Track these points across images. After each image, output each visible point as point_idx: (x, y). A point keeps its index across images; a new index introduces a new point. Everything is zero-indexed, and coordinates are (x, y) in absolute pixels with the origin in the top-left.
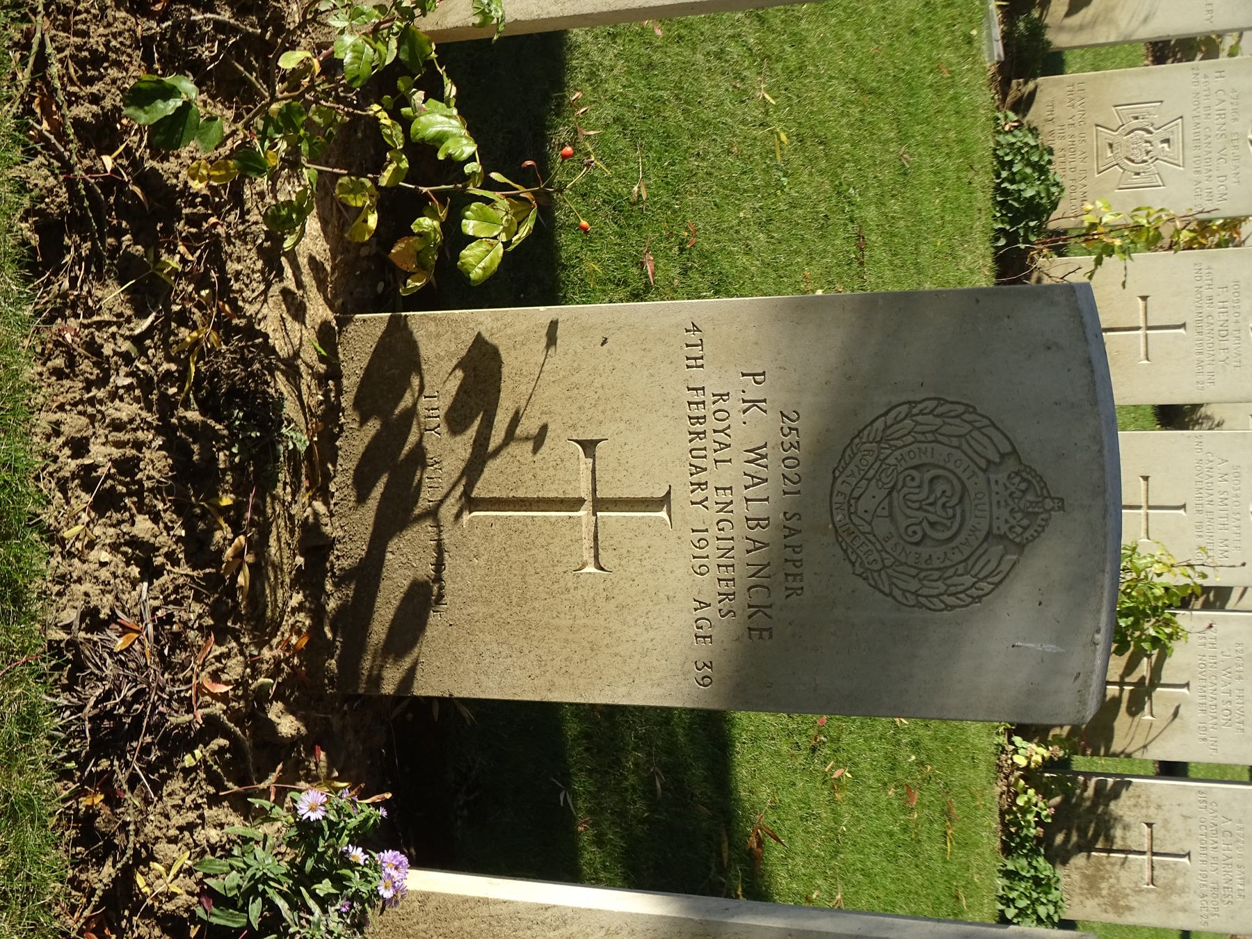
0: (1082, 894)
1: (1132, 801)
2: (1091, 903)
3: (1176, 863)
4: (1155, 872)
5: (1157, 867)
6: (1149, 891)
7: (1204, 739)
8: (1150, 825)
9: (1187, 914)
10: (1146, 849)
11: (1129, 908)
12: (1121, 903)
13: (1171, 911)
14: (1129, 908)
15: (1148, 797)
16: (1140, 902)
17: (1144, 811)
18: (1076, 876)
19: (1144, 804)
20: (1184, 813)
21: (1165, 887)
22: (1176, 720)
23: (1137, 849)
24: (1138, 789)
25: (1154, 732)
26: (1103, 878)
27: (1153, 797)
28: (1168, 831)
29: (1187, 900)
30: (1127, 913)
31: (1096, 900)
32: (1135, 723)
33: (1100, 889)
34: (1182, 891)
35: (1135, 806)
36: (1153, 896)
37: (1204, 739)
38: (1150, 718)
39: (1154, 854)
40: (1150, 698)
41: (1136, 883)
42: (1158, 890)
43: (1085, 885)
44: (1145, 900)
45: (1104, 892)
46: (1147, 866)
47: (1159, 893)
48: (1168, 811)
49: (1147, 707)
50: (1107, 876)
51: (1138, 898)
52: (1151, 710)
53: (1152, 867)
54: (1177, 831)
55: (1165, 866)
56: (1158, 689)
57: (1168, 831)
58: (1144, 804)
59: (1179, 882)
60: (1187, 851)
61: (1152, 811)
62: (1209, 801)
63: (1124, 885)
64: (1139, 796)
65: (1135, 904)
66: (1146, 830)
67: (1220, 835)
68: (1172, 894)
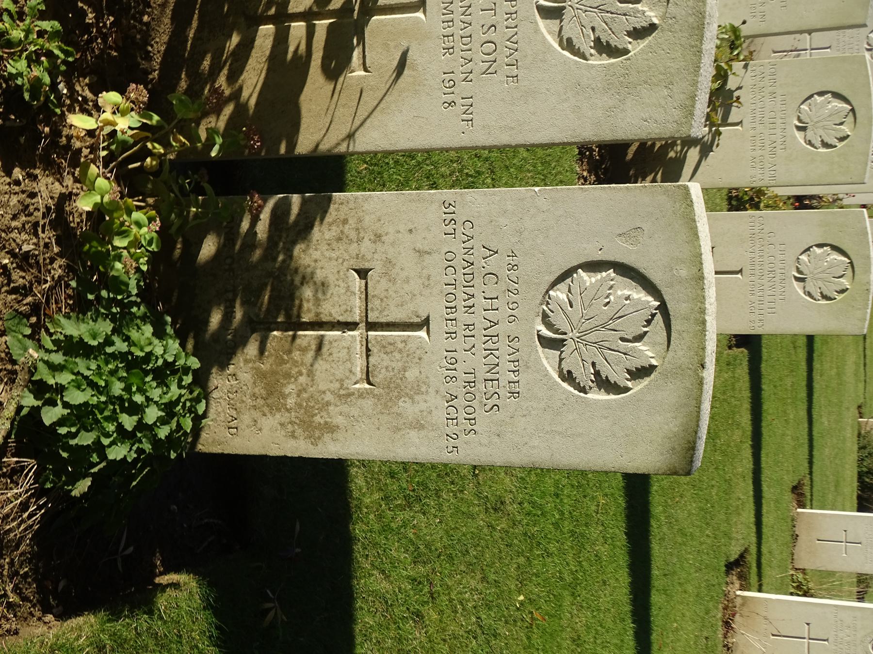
0: (255, 407)
1: (335, 231)
2: (270, 422)
3: (405, 341)
4: (370, 359)
5: (374, 350)
6: (361, 395)
7: (451, 104)
8: (363, 273)
9: (423, 433)
10: (357, 319)
11: (331, 428)
12: (317, 419)
13: (397, 429)
14: (331, 428)
15: (360, 220)
16: (347, 416)
17: (353, 248)
18: (246, 376)
19: (353, 235)
20: (419, 246)
21: (388, 386)
22: (406, 72)
23: (342, 319)
24: (344, 208)
25: (369, 101)
26: (288, 376)
27: (367, 219)
28: (393, 281)
29: (423, 406)
30: (327, 437)
31: (278, 416)
32: (339, 87)
33: (284, 396)
34: (417, 390)
35: (339, 239)
36: (368, 404)
37: (451, 104)
38: (363, 73)
39: (372, 326)
40: (362, 39)
41: (341, 381)
42: (377, 391)
43: (259, 390)
44: (355, 412)
45: (291, 402)
46: (359, 349)
47: (378, 397)
48: (393, 244)
49: (356, 54)
50: (294, 371)
51: (345, 408)
52: (364, 57)
53: (368, 350)
54: (407, 280)
55: (387, 347)
56: (375, 18)
57: (393, 281)
58: (353, 235)
59: (411, 374)
60: (424, 316)
61: (367, 246)
62: (460, 219)
63: (322, 387)
64: (345, 222)
65: (339, 420)
66: (357, 282)
67: (478, 281)
68: (399, 397)
